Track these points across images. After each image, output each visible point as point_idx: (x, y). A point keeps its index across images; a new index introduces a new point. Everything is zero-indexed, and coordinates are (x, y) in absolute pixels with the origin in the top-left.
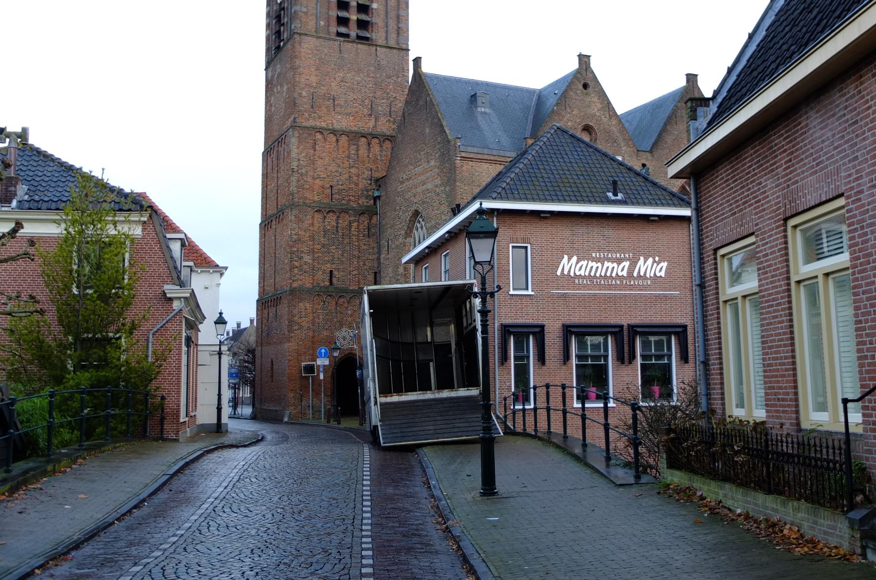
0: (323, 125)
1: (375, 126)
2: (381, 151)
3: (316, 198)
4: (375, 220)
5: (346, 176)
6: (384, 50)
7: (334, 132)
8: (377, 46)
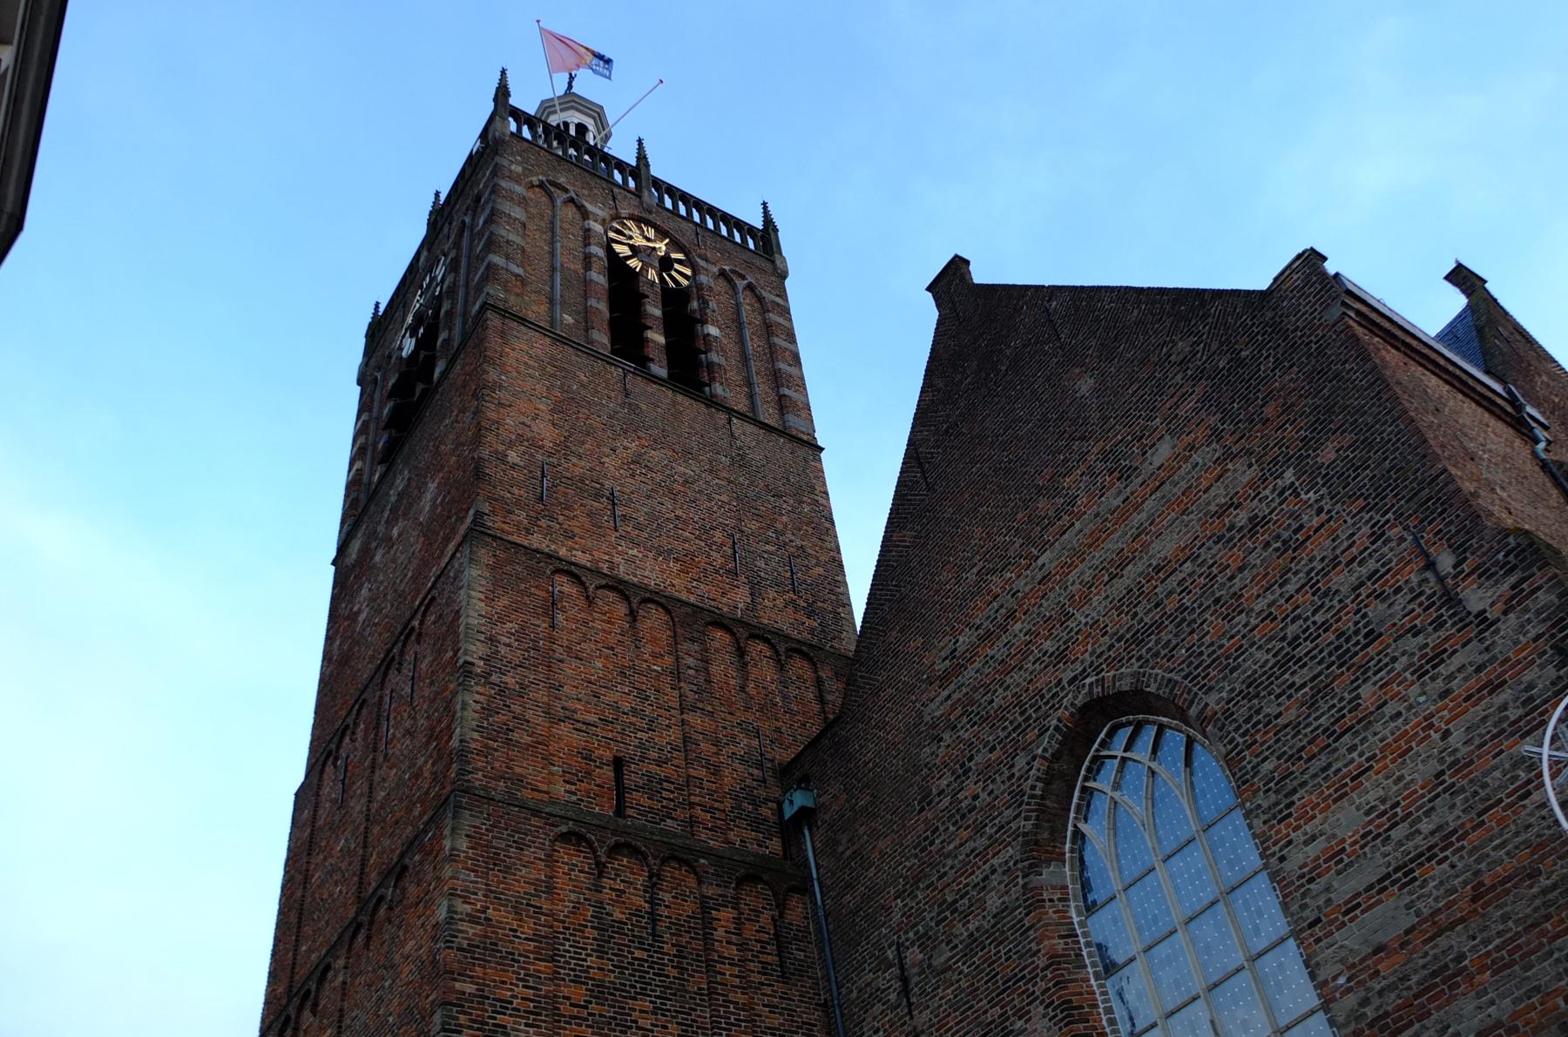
0: (581, 558)
1: (752, 606)
2: (784, 683)
3: (560, 789)
4: (796, 912)
5: (674, 735)
6: (750, 428)
7: (618, 587)
8: (730, 411)
